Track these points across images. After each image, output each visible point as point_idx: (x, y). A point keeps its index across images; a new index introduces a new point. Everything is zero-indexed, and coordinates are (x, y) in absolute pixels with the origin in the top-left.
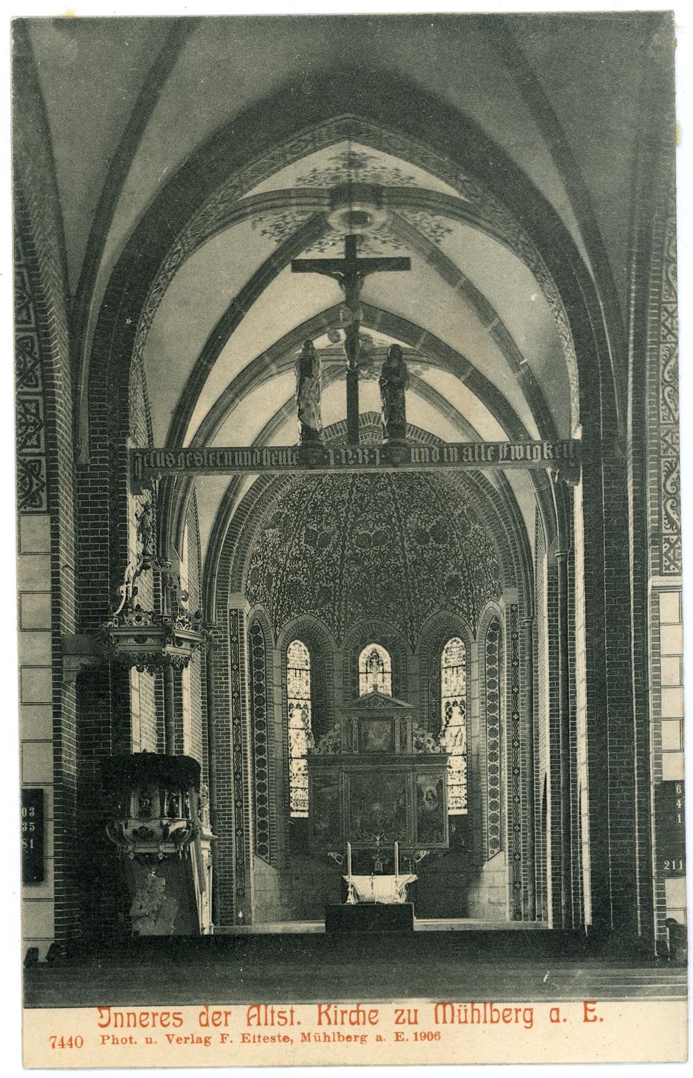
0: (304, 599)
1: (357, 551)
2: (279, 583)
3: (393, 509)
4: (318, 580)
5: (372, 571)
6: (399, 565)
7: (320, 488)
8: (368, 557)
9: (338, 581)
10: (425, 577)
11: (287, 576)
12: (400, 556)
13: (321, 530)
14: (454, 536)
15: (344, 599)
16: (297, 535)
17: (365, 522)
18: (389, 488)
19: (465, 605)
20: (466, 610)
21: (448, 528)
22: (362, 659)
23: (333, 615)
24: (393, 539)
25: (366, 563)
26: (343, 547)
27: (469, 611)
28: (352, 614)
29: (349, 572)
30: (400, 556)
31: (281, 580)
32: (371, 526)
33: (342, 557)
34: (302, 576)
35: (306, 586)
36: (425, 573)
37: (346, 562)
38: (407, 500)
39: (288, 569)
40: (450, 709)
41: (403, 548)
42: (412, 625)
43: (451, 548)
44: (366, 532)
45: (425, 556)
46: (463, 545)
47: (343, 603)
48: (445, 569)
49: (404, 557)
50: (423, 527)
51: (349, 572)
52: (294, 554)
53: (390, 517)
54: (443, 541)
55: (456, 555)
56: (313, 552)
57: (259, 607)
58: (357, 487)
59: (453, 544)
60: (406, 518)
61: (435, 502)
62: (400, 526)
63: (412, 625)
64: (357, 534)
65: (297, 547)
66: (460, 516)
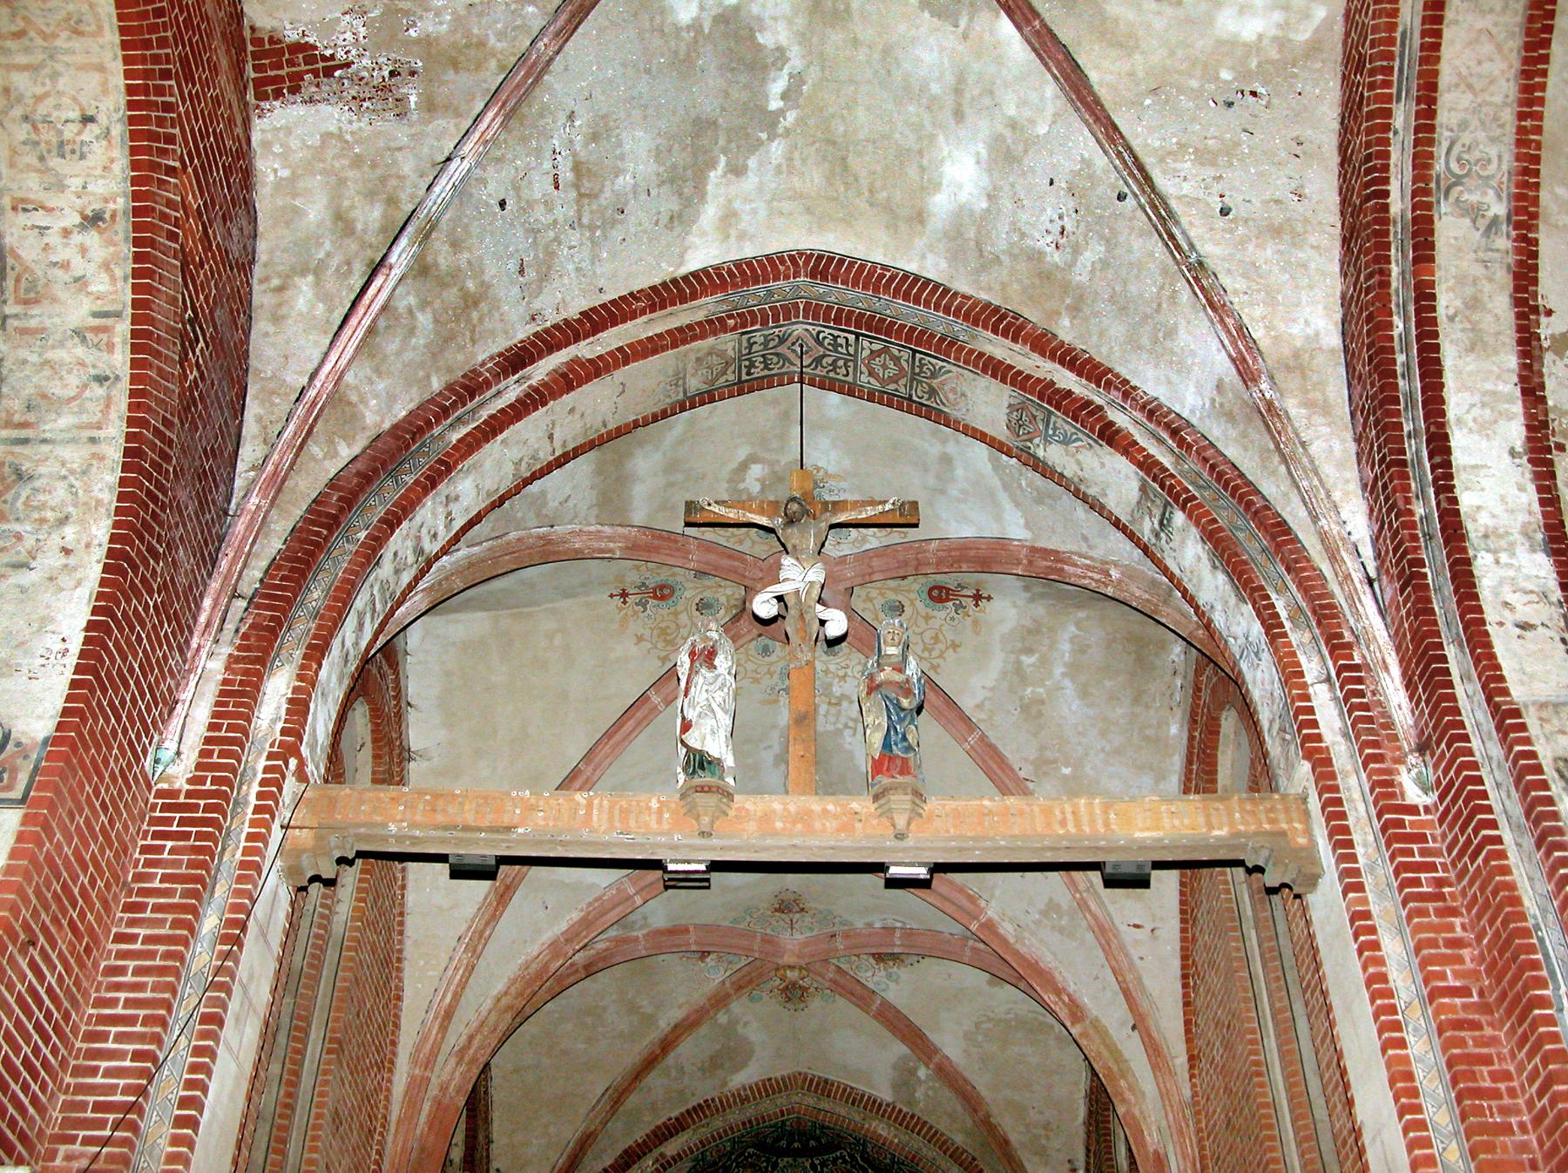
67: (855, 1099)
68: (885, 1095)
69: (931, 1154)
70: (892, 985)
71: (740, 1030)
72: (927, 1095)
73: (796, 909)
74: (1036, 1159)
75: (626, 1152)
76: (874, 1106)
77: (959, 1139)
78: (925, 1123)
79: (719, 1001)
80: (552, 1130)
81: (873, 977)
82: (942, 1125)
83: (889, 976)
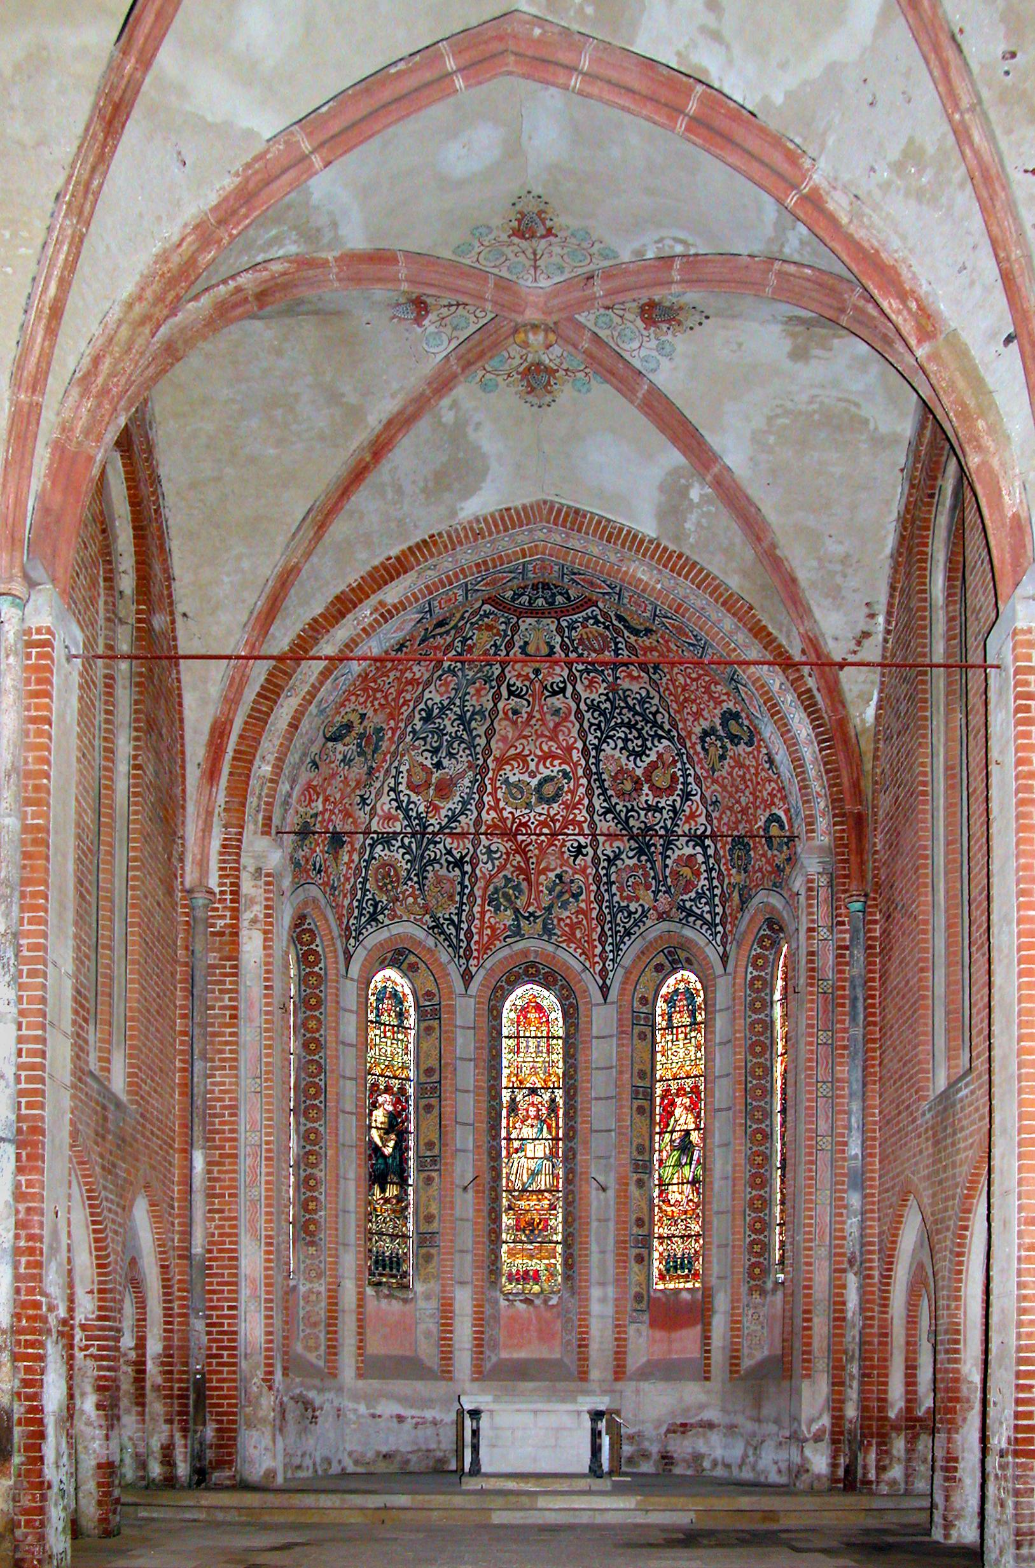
0: (403, 893)
1: (505, 814)
2: (355, 857)
3: (574, 733)
4: (431, 862)
5: (533, 850)
8: (525, 825)
9: (468, 868)
10: (631, 862)
12: (585, 825)
13: (439, 765)
14: (690, 779)
15: (479, 901)
17: (521, 758)
19: (707, 908)
20: (708, 917)
21: (679, 765)
22: (508, 1014)
23: (458, 928)
24: (573, 792)
27: (714, 919)
28: (492, 927)
29: (489, 851)
31: (361, 854)
32: (532, 766)
33: (478, 822)
34: (402, 851)
36: (631, 854)
38: (603, 713)
40: (673, 1104)
41: (590, 808)
44: (522, 777)
45: (632, 822)
46: (707, 795)
47: (476, 909)
48: (668, 845)
50: (631, 765)
51: (489, 851)
52: (386, 808)
53: (570, 749)
54: (670, 790)
55: (692, 816)
56: (422, 809)
57: (314, 891)
58: (509, 685)
59: (687, 796)
60: (598, 749)
61: (658, 712)
62: (587, 768)
66: (706, 733)
67: (610, 533)
68: (648, 528)
69: (699, 603)
70: (665, 363)
71: (472, 435)
72: (699, 524)
73: (541, 231)
74: (827, 602)
75: (337, 598)
76: (634, 542)
77: (734, 583)
78: (695, 564)
79: (442, 384)
80: (246, 564)
81: (639, 347)
82: (714, 565)
83: (660, 348)
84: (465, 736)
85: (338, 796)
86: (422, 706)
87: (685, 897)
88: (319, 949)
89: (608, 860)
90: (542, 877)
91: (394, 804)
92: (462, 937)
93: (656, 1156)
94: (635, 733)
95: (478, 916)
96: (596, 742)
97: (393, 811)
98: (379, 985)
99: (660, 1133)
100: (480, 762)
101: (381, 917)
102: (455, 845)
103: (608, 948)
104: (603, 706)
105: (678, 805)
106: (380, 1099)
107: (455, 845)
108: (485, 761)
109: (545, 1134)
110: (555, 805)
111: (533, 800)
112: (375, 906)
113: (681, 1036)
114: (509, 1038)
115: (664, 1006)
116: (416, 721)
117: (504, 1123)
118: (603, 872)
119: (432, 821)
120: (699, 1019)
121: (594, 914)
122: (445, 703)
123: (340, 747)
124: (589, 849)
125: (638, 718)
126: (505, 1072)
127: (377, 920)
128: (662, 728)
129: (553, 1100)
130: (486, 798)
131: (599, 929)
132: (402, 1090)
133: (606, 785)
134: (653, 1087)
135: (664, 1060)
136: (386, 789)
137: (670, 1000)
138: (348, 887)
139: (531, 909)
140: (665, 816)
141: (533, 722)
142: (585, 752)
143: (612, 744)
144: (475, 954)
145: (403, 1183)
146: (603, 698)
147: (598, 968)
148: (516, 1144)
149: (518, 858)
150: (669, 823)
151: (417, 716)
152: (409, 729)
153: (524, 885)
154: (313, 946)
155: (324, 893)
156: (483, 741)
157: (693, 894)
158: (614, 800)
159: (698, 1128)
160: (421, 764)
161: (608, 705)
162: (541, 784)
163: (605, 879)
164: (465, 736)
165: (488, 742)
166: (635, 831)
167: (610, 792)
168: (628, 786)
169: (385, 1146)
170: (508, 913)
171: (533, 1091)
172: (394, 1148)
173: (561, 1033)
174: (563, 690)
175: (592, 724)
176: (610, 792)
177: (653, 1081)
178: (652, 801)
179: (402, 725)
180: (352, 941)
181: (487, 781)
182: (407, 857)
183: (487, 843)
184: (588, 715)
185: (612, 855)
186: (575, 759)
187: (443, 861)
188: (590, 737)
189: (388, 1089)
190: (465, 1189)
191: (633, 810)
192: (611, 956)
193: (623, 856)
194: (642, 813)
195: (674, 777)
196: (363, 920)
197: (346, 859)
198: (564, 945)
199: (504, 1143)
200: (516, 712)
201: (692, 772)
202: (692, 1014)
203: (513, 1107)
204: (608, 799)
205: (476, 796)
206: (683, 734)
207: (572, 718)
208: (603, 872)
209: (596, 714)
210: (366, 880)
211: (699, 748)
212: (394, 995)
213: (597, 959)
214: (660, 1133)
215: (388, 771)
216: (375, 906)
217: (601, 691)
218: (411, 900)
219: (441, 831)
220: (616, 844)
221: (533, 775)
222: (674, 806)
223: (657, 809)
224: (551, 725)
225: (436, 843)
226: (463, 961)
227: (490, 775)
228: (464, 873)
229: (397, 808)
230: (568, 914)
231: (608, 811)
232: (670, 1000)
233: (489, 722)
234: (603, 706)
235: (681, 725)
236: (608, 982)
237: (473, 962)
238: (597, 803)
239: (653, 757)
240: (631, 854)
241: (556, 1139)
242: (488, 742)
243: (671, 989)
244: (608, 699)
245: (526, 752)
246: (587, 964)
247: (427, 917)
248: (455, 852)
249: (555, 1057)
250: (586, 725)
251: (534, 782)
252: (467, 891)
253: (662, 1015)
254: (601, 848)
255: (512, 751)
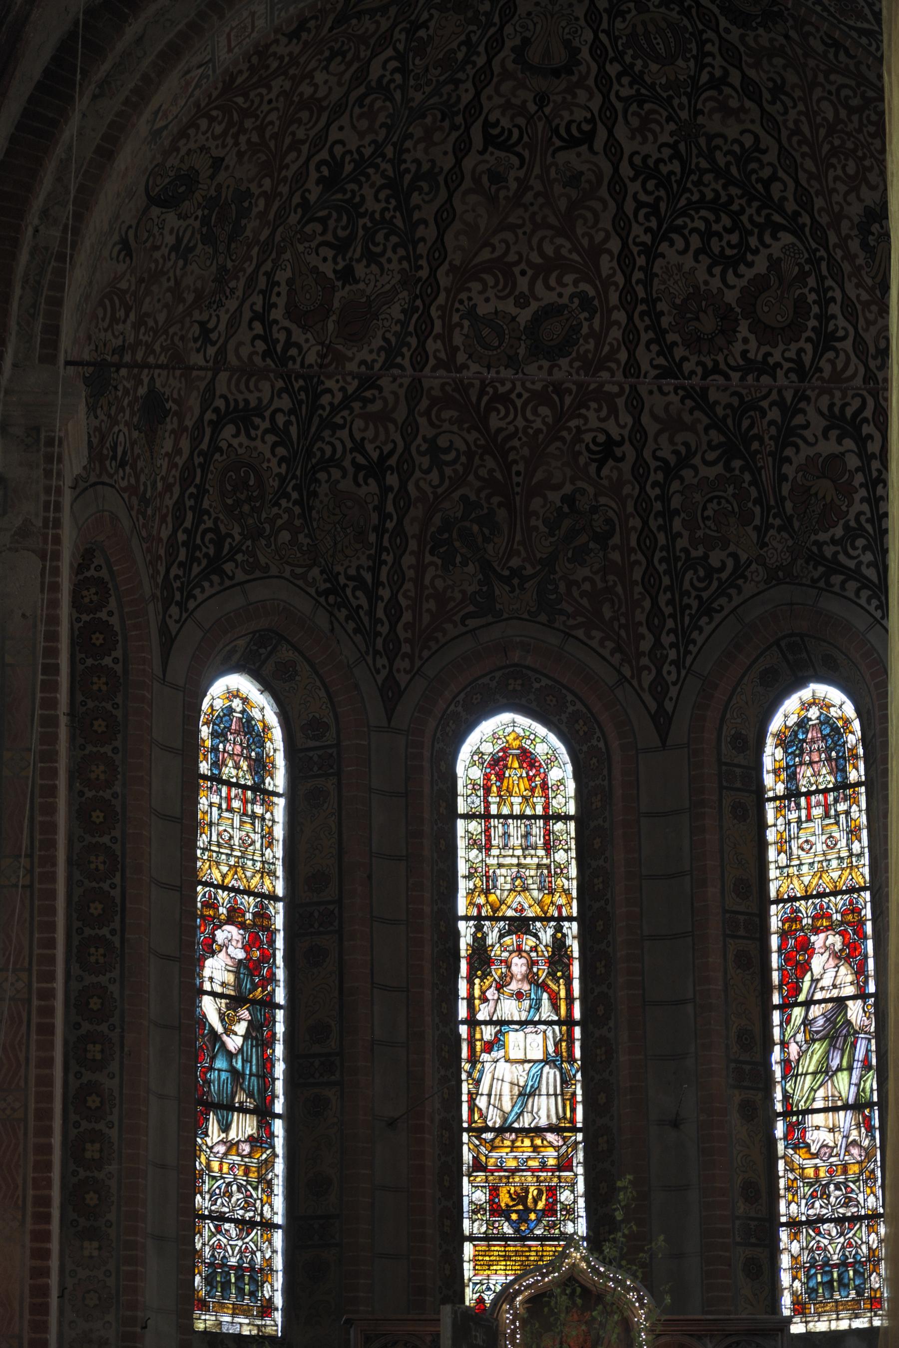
2: (185, 444)
3: (606, 222)
6: (615, 432)
7: (360, 101)
8: (505, 399)
9: (392, 480)
11: (217, 426)
12: (620, 402)
13: (347, 275)
14: (834, 309)
15: (413, 545)
16: (262, 282)
18: (602, 134)
19: (868, 557)
21: (812, 282)
22: (467, 769)
25: (494, 422)
26: (420, 359)
30: (620, 402)
32: (523, 284)
33: (415, 391)
34: (271, 439)
35: (282, 479)
36: (711, 456)
37: (427, 413)
39: (220, 403)
40: (806, 948)
41: (632, 368)
42: (658, 644)
43: (817, 355)
44: (501, 306)
45: (713, 395)
47: (408, 560)
48: (788, 435)
49: (636, 404)
50: (716, 283)
52: (245, 352)
56: (311, 358)
58: (486, 124)
60: (651, 253)
61: (774, 178)
63: (658, 644)
64: (471, 313)
65: (258, 328)
84: (399, 222)
85: (162, 317)
86: (324, 155)
87: (822, 537)
88: (115, 621)
89: (665, 467)
90: (536, 503)
91: (260, 346)
92: (380, 613)
93: (777, 1055)
94: (726, 221)
95: (410, 573)
96: (647, 239)
97: (257, 360)
98: (218, 704)
99: (782, 1007)
100: (424, 273)
101: (228, 567)
102: (370, 434)
103: (667, 639)
104: (664, 169)
105: (807, 359)
106: (220, 936)
107: (370, 434)
108: (433, 272)
109: (546, 1012)
110: (564, 362)
111: (522, 351)
112: (219, 543)
113: (817, 812)
114: (468, 817)
115: (779, 753)
116: (311, 184)
117: (463, 987)
118: (654, 493)
119: (330, 384)
120: (853, 776)
121: (637, 575)
122: (367, 152)
123: (171, 219)
124: (627, 448)
125: (734, 191)
126: (463, 885)
127: (222, 573)
128: (781, 211)
129: (559, 945)
130: (432, 346)
131: (647, 604)
132: (262, 915)
133: (665, 321)
134: (765, 917)
135: (783, 859)
136: (247, 315)
137: (790, 741)
138: (169, 502)
139: (515, 562)
140: (782, 381)
141: (529, 197)
142: (625, 260)
143: (680, 243)
144: (406, 648)
145: (264, 1114)
146: (667, 152)
147: (647, 678)
148: (488, 1033)
149: (490, 463)
150: (788, 396)
151: (314, 175)
152: (297, 199)
153: (502, 514)
154: (103, 615)
155: (130, 508)
156: (429, 233)
157: (839, 532)
158: (679, 352)
159: (862, 995)
160: (315, 270)
161: (676, 166)
162: (537, 320)
163: (658, 506)
164: (399, 222)
165: (440, 236)
166: (720, 411)
167: (671, 337)
168: (709, 324)
169: (229, 1031)
170: (471, 568)
171: (520, 925)
172: (245, 1037)
173: (571, 809)
174: (589, 138)
175: (640, 205)
176: (671, 337)
177: (765, 902)
178: (755, 351)
179: (284, 189)
180: (174, 610)
181: (434, 313)
182: (281, 451)
183: (430, 432)
184: (634, 187)
185: (672, 460)
186: (605, 271)
187: (347, 463)
188: (636, 230)
189: (234, 916)
190: (392, 1124)
191: (716, 370)
192: (672, 654)
193: (697, 460)
194: (735, 376)
195: (801, 305)
196: (196, 569)
197: (168, 445)
198: (580, 633)
199: (463, 1030)
200: (496, 177)
201: (838, 294)
202: (839, 769)
203: (481, 958)
204: (666, 350)
205: (413, 341)
206: (824, 220)
207: (603, 192)
208: (654, 493)
209: (650, 185)
210: (202, 491)
211: (854, 245)
212: (248, 726)
213: (645, 661)
214: (782, 1007)
215: (252, 280)
216: (219, 543)
217: (665, 138)
218: (285, 536)
219: (346, 402)
220: (679, 438)
221: (522, 302)
222: (799, 362)
223: (766, 368)
224: (563, 204)
225: (335, 427)
226: (382, 661)
227: (441, 299)
228: (385, 490)
229: (266, 354)
230: (586, 572)
231: (665, 373)
232: (790, 741)
233: (443, 193)
234: (664, 169)
235: (819, 202)
236: (669, 706)
237: (402, 664)
238: (644, 358)
239: (761, 265)
240: (711, 456)
241: (569, 1022)
242: (440, 236)
243: (792, 720)
244: (676, 155)
245: (512, 257)
246: (627, 671)
247: (316, 571)
248: (369, 447)
249: (560, 856)
250: (629, 206)
251: (525, 316)
252: (390, 525)
253: (776, 772)
254: (651, 445)
255: (486, 255)
